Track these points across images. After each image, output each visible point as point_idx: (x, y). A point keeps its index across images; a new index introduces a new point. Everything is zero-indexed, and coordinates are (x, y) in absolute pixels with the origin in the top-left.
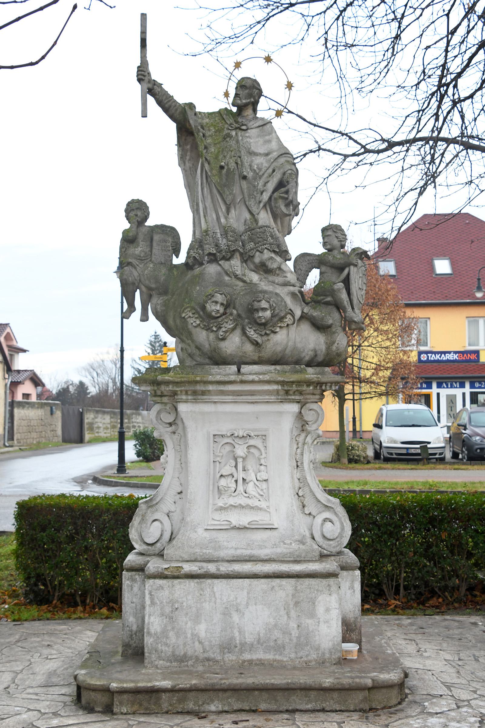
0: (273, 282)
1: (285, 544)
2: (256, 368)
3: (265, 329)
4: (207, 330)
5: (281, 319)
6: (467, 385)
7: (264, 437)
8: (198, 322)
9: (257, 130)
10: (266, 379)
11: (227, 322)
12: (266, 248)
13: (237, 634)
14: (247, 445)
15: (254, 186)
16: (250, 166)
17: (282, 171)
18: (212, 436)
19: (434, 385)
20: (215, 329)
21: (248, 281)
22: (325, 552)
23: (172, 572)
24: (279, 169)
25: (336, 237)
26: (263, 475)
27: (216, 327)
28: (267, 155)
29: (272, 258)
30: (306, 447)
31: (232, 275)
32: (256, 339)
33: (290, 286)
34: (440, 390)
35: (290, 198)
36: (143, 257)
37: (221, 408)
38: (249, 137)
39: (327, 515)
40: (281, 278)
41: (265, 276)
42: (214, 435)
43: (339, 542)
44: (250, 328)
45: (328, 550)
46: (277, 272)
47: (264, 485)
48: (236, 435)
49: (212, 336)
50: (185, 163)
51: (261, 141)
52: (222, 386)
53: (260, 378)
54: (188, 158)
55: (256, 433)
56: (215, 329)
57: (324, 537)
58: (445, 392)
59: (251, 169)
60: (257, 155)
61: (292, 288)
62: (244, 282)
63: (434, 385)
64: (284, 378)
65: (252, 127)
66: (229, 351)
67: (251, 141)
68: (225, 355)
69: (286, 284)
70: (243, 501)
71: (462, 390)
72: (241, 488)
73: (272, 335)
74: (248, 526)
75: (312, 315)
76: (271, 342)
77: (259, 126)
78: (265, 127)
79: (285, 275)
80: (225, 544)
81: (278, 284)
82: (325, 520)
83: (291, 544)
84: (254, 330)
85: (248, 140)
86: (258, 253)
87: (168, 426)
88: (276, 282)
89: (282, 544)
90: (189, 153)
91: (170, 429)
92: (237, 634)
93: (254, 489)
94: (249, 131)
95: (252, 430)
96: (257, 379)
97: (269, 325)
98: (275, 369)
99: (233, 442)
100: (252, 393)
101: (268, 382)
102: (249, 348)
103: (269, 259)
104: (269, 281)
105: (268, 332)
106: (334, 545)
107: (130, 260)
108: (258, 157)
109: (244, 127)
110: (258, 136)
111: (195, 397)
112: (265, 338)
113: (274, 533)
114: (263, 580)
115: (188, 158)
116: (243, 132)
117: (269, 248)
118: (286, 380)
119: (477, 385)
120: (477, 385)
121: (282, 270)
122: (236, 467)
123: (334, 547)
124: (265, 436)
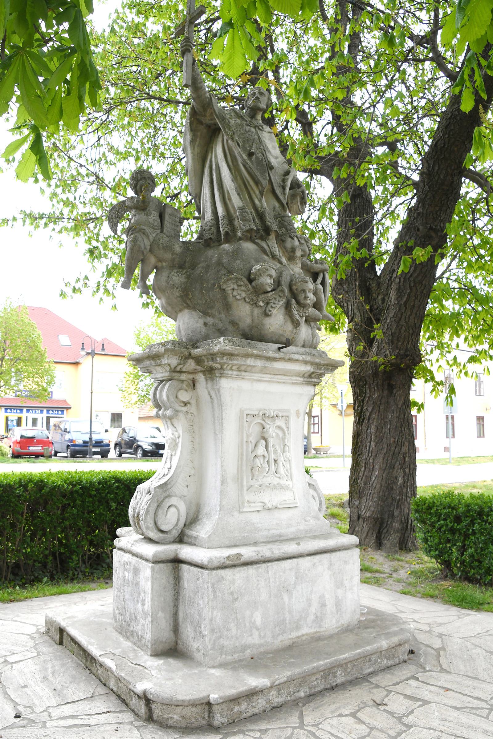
1: (305, 521)
4: (252, 305)
6: (45, 411)
8: (244, 295)
11: (275, 299)
13: (287, 615)
19: (25, 410)
20: (261, 304)
23: (232, 560)
27: (263, 301)
31: (269, 254)
34: (28, 415)
37: (261, 386)
42: (247, 415)
48: (267, 415)
49: (256, 311)
50: (194, 147)
52: (269, 363)
54: (197, 143)
56: (261, 304)
58: (31, 416)
63: (25, 410)
66: (272, 329)
68: (266, 332)
70: (276, 481)
71: (42, 415)
72: (273, 468)
80: (259, 525)
86: (289, 239)
87: (183, 405)
90: (198, 140)
91: (184, 409)
95: (280, 410)
96: (301, 358)
99: (263, 422)
100: (286, 373)
107: (143, 227)
111: (239, 373)
115: (197, 143)
119: (51, 412)
120: (51, 412)
122: (267, 447)
124: (288, 417)
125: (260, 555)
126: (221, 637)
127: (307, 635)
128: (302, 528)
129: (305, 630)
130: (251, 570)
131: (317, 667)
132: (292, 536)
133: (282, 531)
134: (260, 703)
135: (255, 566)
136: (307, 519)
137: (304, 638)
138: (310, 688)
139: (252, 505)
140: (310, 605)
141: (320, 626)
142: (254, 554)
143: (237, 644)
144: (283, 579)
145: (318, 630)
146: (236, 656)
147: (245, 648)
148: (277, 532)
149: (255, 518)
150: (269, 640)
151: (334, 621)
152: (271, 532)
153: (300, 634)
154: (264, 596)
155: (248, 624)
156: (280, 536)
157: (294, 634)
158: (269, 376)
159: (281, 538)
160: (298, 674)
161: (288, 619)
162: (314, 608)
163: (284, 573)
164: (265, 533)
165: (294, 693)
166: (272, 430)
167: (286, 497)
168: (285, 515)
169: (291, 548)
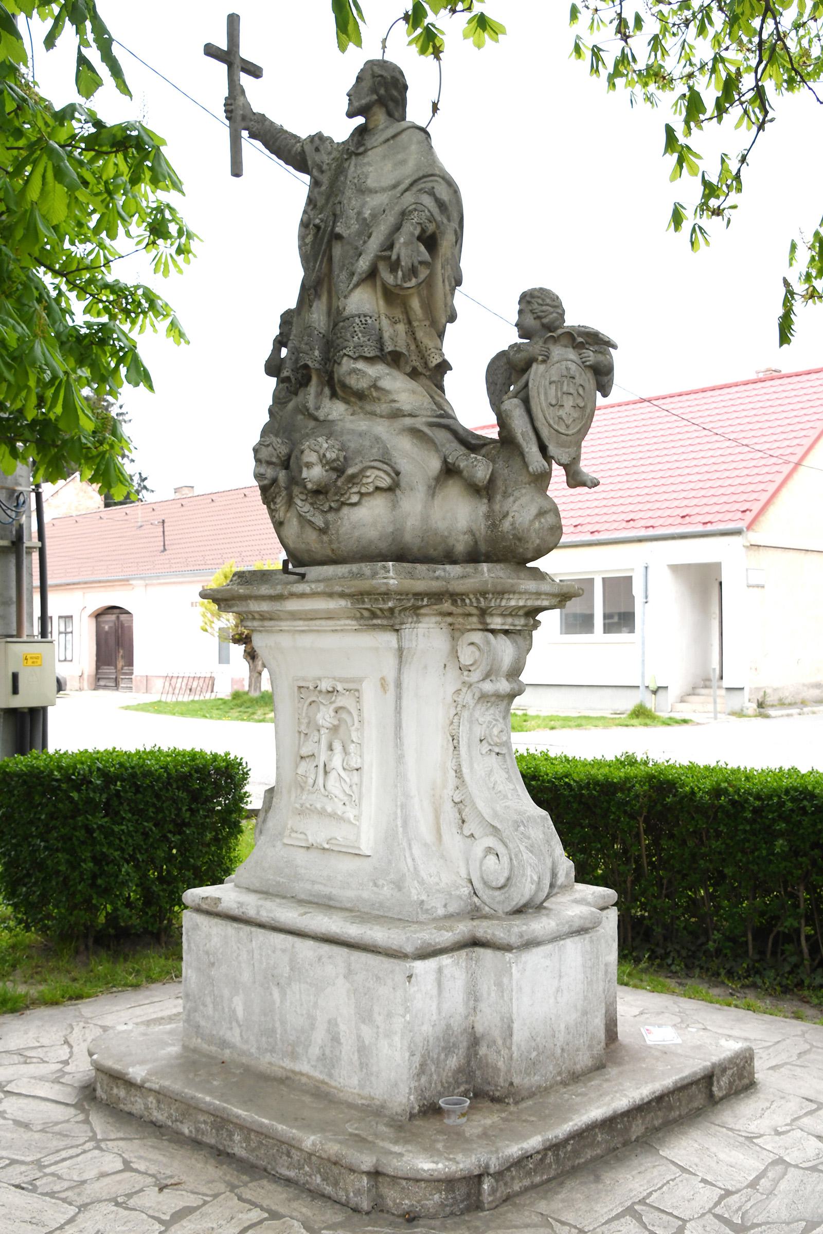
0: (373, 414)
1: (375, 885)
2: (329, 570)
3: (328, 500)
5: (352, 479)
7: (357, 694)
9: (386, 146)
10: (319, 590)
12: (345, 354)
14: (334, 706)
15: (357, 248)
16: (359, 213)
17: (397, 209)
18: (296, 689)
21: (322, 418)
22: (487, 909)
24: (392, 208)
25: (531, 311)
26: (354, 762)
28: (394, 187)
29: (354, 371)
30: (466, 714)
32: (312, 519)
33: (404, 416)
35: (394, 257)
36: (284, 398)
38: (369, 164)
39: (490, 841)
40: (384, 405)
41: (360, 404)
43: (507, 895)
44: (302, 500)
45: (492, 906)
46: (375, 394)
47: (355, 776)
51: (389, 166)
52: (278, 604)
53: (311, 589)
55: (347, 686)
57: (485, 883)
59: (357, 220)
60: (376, 192)
61: (408, 421)
62: (316, 419)
64: (343, 586)
65: (375, 144)
67: (371, 169)
69: (396, 414)
73: (345, 510)
74: (327, 846)
75: (459, 466)
76: (346, 522)
77: (388, 140)
78: (399, 138)
79: (391, 397)
80: (303, 871)
81: (382, 417)
82: (489, 850)
83: (383, 885)
84: (311, 504)
85: (365, 170)
88: (378, 411)
89: (371, 884)
92: (278, 1024)
93: (337, 785)
94: (370, 153)
95: (341, 680)
97: (330, 494)
98: (350, 572)
101: (331, 595)
102: (311, 536)
103: (350, 374)
104: (367, 413)
105: (333, 505)
106: (498, 899)
108: (378, 195)
109: (361, 149)
110: (384, 157)
112: (331, 517)
113: (365, 864)
114: (310, 943)
116: (360, 157)
117: (350, 353)
118: (347, 591)
121: (383, 389)
123: (499, 903)
124: (357, 690)
125: (241, 910)
126: (196, 1011)
127: (309, 1077)
128: (365, 895)
129: (304, 1067)
130: (230, 929)
131: (198, 1099)
132: (349, 905)
133: (334, 892)
134: (137, 1105)
135: (235, 925)
136: (381, 882)
137: (304, 1080)
138: (198, 1130)
139: (294, 835)
140: (313, 1027)
141: (330, 1075)
142: (235, 906)
143: (214, 1032)
144: (272, 962)
145: (327, 1079)
146: (213, 1049)
147: (224, 1044)
148: (326, 890)
149: (301, 857)
150: (253, 1050)
151: (355, 1081)
152: (317, 887)
153: (297, 1069)
154: (246, 977)
155: (226, 1010)
156: (330, 898)
157: (288, 1064)
158: (301, 623)
159: (331, 903)
160: (173, 1092)
161: (279, 1031)
162: (319, 1036)
163: (274, 952)
164: (308, 886)
165: (176, 1121)
166: (325, 717)
167: (341, 834)
168: (347, 865)
169: (289, 915)
